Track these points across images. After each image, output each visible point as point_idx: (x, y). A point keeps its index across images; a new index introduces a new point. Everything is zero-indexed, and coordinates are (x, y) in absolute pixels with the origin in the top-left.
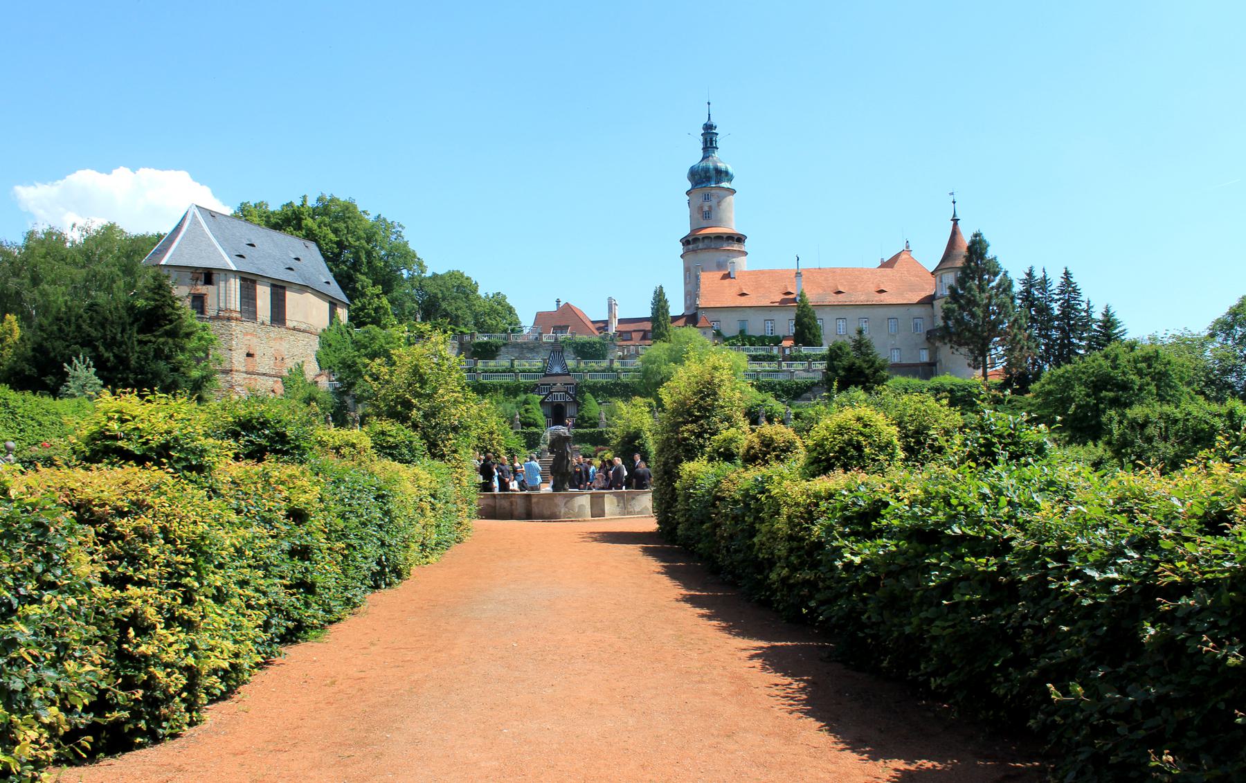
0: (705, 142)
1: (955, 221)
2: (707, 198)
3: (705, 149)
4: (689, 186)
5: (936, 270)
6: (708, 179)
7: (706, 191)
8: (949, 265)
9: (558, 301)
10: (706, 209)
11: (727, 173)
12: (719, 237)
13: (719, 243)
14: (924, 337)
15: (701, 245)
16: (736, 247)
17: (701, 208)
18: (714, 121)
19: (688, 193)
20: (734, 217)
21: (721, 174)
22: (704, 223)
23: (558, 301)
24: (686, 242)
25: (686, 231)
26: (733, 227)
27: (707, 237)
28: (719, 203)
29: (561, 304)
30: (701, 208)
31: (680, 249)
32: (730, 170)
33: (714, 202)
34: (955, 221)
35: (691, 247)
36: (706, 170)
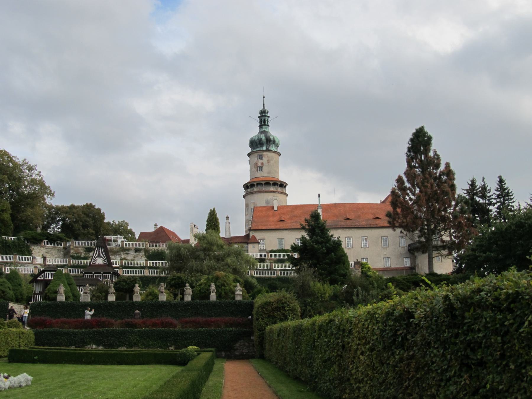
0: (261, 121)
2: (260, 157)
3: (261, 127)
4: (250, 150)
9: (156, 225)
10: (260, 165)
11: (274, 142)
12: (267, 184)
14: (406, 249)
15: (255, 189)
16: (279, 189)
17: (256, 164)
19: (249, 155)
21: (270, 141)
23: (156, 225)
24: (246, 186)
25: (247, 180)
27: (259, 184)
29: (158, 227)
30: (256, 164)
31: (243, 191)
33: (265, 160)
35: (249, 190)
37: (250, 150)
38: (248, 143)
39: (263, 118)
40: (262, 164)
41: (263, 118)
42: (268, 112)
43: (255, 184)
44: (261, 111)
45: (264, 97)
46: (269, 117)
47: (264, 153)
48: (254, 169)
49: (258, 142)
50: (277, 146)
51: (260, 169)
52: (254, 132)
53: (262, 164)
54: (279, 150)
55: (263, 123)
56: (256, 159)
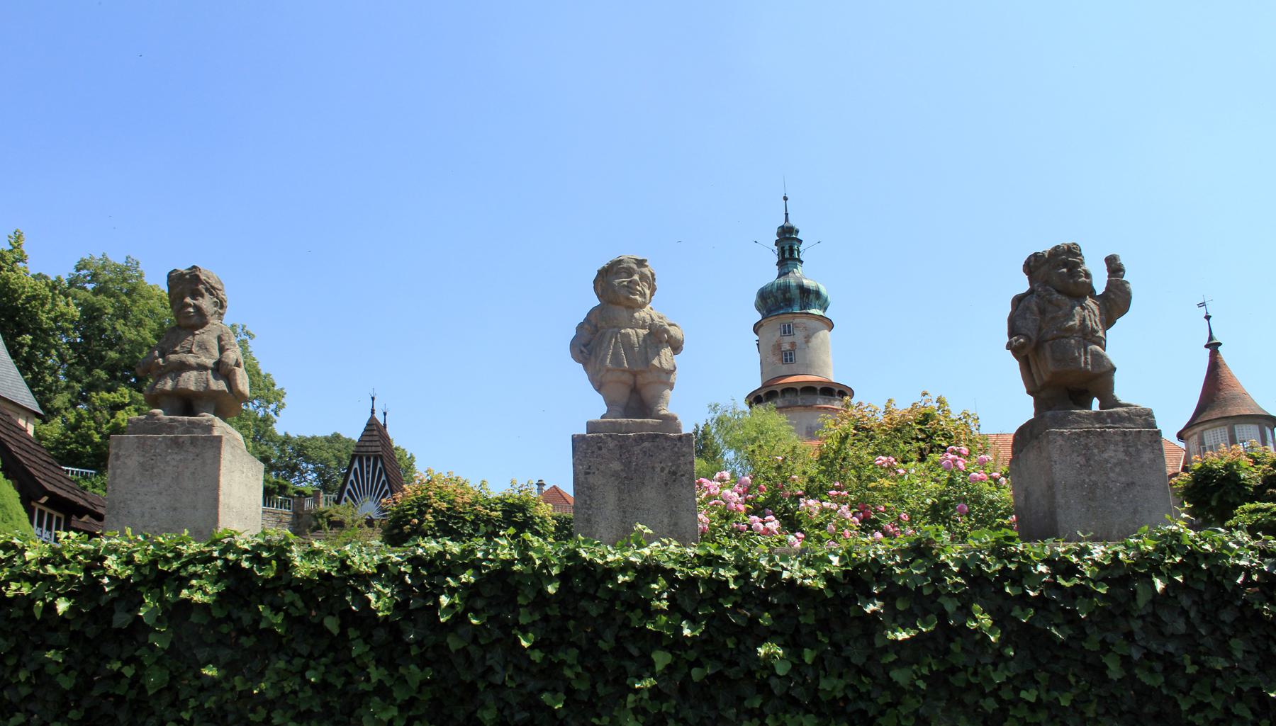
0: (782, 252)
1: (1213, 346)
2: (787, 330)
4: (758, 317)
5: (1190, 425)
6: (789, 302)
7: (787, 319)
8: (1216, 414)
10: (786, 347)
11: (818, 294)
12: (809, 389)
13: (809, 399)
17: (778, 346)
18: (793, 222)
19: (757, 328)
20: (833, 359)
21: (809, 296)
22: (784, 369)
26: (833, 374)
27: (790, 390)
28: (808, 339)
30: (778, 346)
32: (823, 290)
33: (798, 336)
34: (1213, 346)
36: (785, 289)
37: (758, 317)
38: (753, 297)
39: (788, 245)
40: (793, 344)
41: (788, 245)
42: (797, 232)
43: (779, 390)
44: (782, 227)
45: (785, 199)
46: (800, 241)
47: (797, 320)
48: (775, 359)
49: (780, 296)
50: (824, 307)
51: (788, 357)
52: (768, 274)
53: (793, 344)
54: (827, 315)
55: (787, 255)
56: (778, 334)
